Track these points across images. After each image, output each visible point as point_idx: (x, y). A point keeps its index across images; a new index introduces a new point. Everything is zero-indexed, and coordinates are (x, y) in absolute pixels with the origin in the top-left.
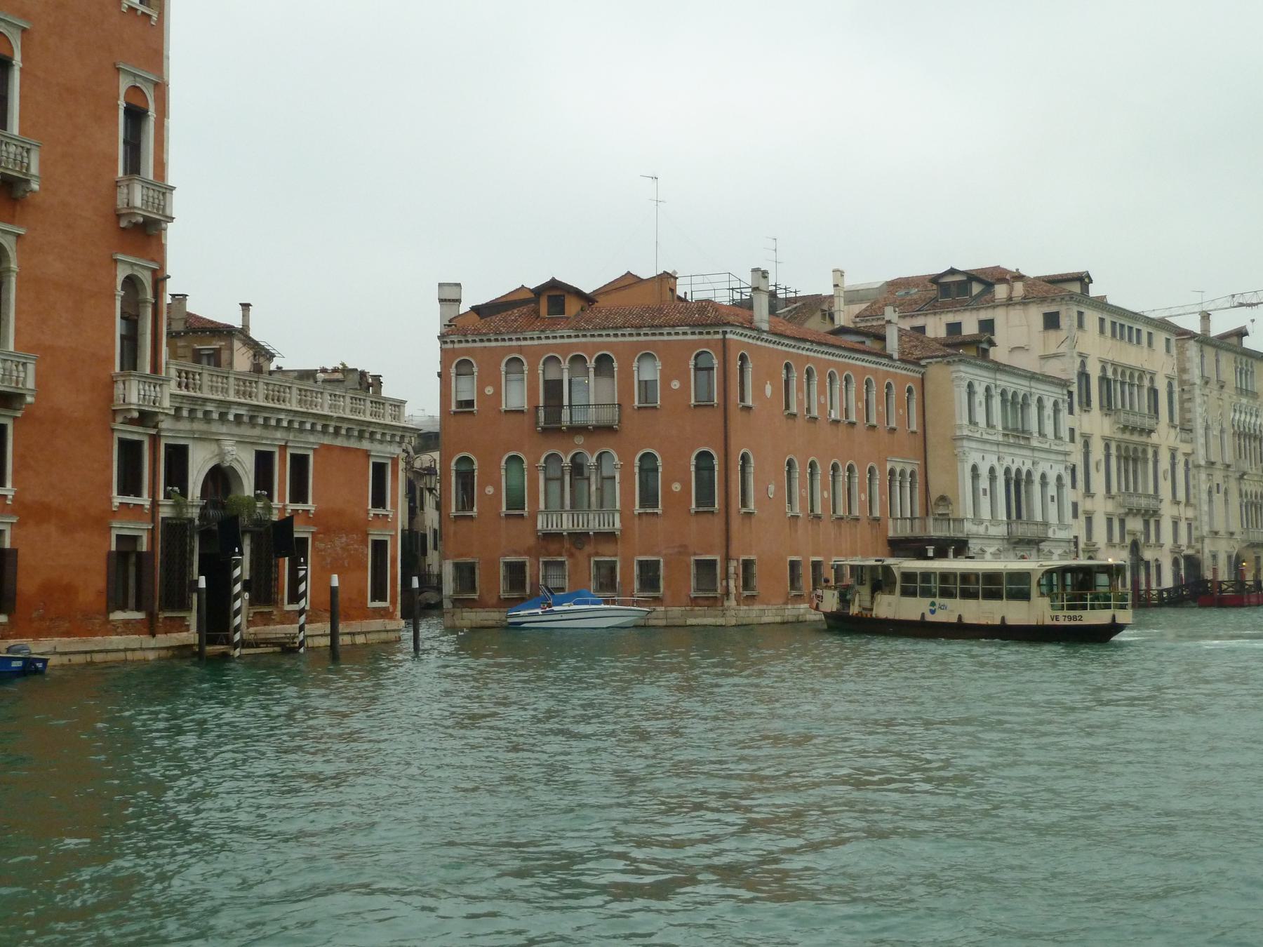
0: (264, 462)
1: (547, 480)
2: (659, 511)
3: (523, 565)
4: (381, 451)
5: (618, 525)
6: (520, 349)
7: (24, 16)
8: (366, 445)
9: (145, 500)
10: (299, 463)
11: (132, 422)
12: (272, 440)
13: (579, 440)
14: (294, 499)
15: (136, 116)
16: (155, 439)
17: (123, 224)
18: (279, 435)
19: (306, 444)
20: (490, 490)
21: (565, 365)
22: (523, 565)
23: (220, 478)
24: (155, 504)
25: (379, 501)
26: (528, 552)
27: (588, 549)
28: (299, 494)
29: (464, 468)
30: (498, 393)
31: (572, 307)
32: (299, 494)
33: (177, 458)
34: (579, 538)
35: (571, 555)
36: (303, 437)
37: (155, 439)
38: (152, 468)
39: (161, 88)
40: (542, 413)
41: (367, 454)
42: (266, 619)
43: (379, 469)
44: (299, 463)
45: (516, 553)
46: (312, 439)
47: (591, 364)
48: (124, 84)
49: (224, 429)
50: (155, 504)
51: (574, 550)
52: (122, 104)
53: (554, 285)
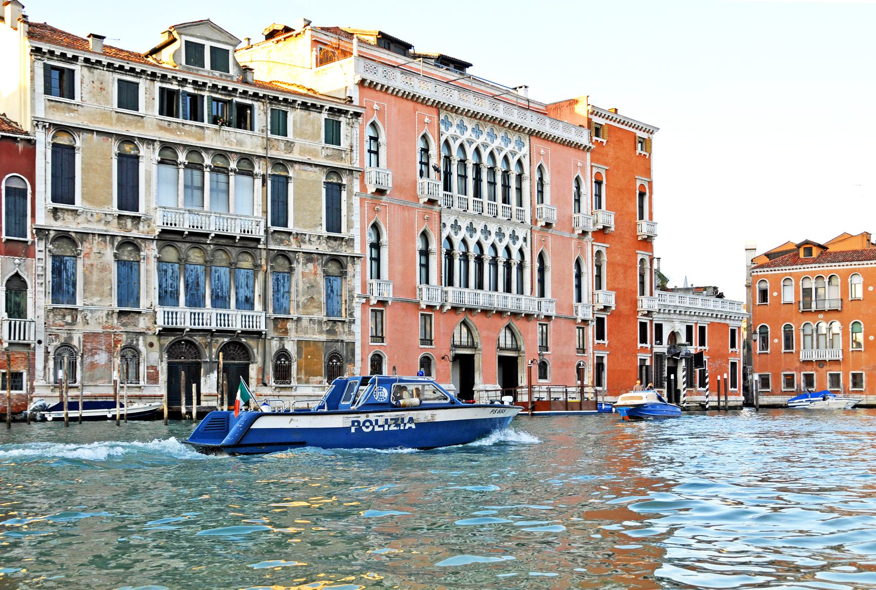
0: (689, 329)
1: (804, 335)
2: (862, 349)
3: (793, 375)
4: (733, 324)
5: (841, 357)
6: (791, 274)
7: (606, 165)
8: (728, 322)
9: (648, 345)
10: (702, 329)
11: (645, 315)
12: (692, 321)
14: (700, 345)
15: (642, 195)
16: (651, 321)
17: (640, 239)
18: (695, 318)
19: (705, 322)
20: (776, 341)
22: (793, 375)
23: (673, 336)
24: (652, 347)
25: (733, 345)
26: (796, 370)
27: (825, 368)
28: (702, 343)
29: (763, 330)
30: (779, 295)
31: (815, 252)
32: (702, 343)
33: (659, 327)
34: (821, 363)
35: (817, 371)
36: (704, 319)
37: (651, 321)
38: (650, 333)
39: (650, 183)
40: (801, 305)
41: (727, 325)
42: (690, 393)
43: (733, 331)
44: (702, 329)
45: (790, 370)
46: (707, 319)
48: (638, 183)
49: (675, 317)
50: (652, 347)
51: (818, 369)
52: (638, 192)
53: (807, 242)
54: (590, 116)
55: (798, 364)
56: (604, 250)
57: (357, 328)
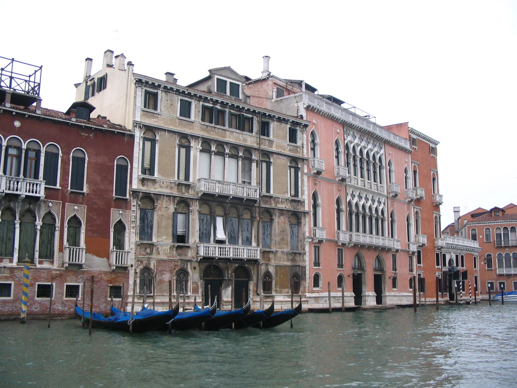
0: (457, 256)
6: (489, 226)
7: (418, 161)
8: (473, 253)
10: (462, 257)
13: (507, 249)
15: (434, 179)
16: (441, 253)
17: (434, 204)
19: (464, 253)
21: (502, 229)
23: (451, 261)
25: (475, 267)
26: (494, 279)
27: (511, 279)
28: (463, 266)
32: (463, 266)
33: (444, 256)
34: (509, 276)
35: (506, 280)
37: (441, 253)
39: (437, 173)
41: (473, 255)
43: (475, 258)
44: (462, 257)
45: (491, 280)
47: (509, 229)
54: (410, 134)
55: (495, 277)
56: (419, 211)
57: (307, 258)
